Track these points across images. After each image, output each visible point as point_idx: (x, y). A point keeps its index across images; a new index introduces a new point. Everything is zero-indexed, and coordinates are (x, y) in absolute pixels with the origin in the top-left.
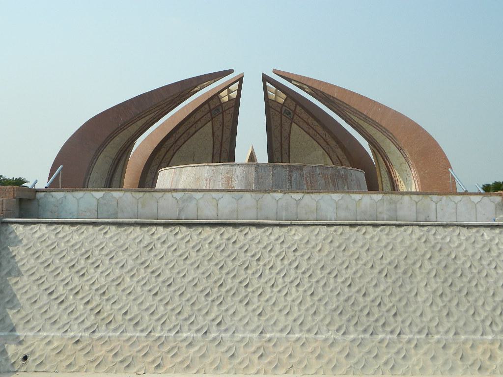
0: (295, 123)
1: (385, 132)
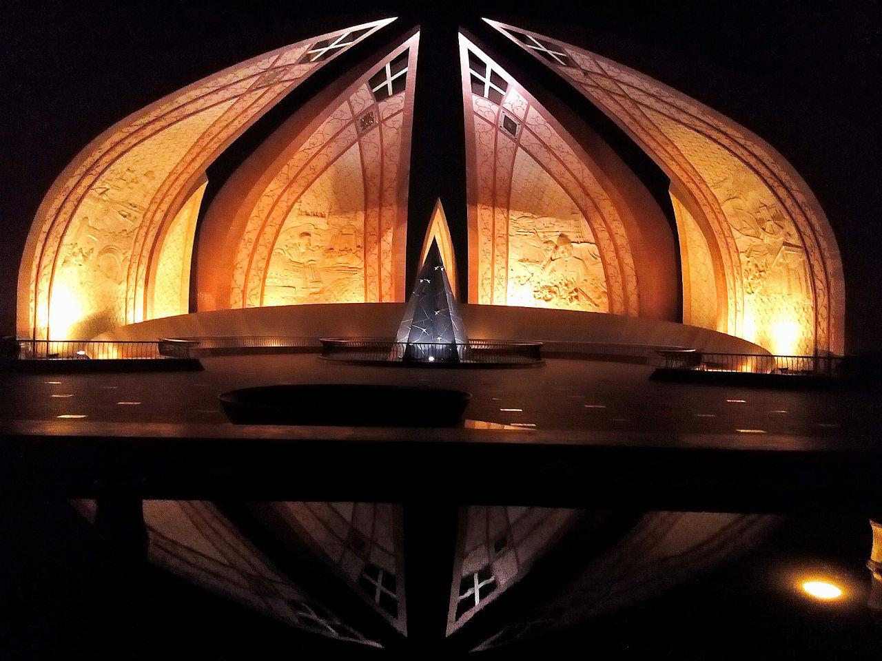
0: (525, 149)
1: (743, 146)
